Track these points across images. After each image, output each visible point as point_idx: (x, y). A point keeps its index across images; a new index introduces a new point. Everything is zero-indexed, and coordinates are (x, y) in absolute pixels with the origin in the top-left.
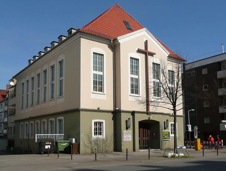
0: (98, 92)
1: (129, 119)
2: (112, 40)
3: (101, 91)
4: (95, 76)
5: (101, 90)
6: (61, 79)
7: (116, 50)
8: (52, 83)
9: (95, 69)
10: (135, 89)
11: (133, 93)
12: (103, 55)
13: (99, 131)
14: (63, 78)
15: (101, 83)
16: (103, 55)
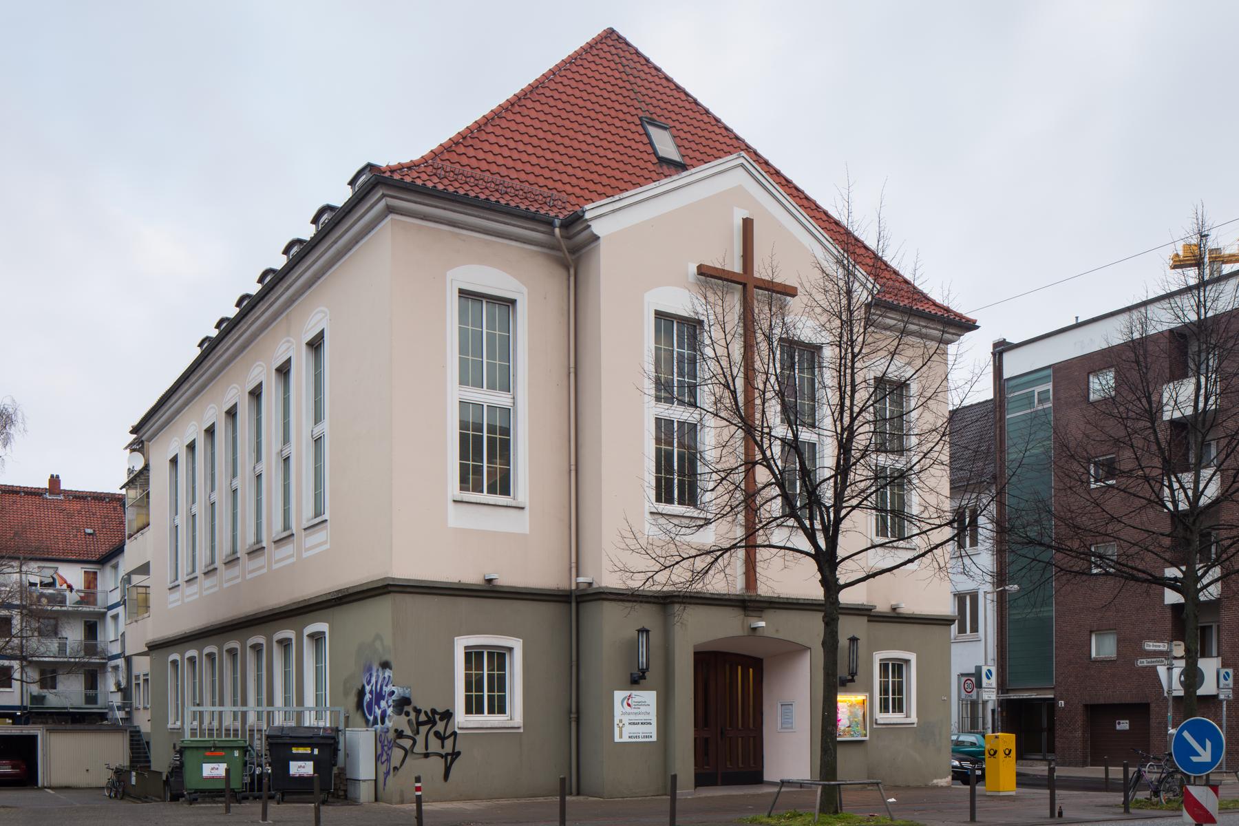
0: (485, 497)
1: (643, 631)
2: (557, 222)
3: (505, 491)
4: (664, 427)
5: (502, 485)
6: (317, 431)
7: (581, 276)
8: (285, 454)
9: (469, 376)
10: (677, 477)
11: (669, 501)
12: (513, 302)
13: (486, 690)
14: (325, 427)
15: (502, 447)
16: (513, 302)
